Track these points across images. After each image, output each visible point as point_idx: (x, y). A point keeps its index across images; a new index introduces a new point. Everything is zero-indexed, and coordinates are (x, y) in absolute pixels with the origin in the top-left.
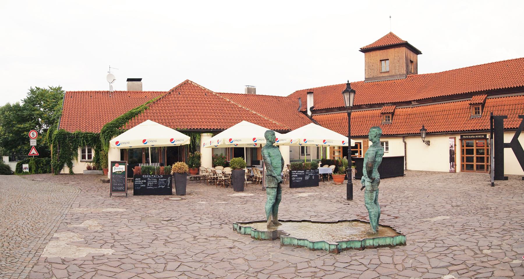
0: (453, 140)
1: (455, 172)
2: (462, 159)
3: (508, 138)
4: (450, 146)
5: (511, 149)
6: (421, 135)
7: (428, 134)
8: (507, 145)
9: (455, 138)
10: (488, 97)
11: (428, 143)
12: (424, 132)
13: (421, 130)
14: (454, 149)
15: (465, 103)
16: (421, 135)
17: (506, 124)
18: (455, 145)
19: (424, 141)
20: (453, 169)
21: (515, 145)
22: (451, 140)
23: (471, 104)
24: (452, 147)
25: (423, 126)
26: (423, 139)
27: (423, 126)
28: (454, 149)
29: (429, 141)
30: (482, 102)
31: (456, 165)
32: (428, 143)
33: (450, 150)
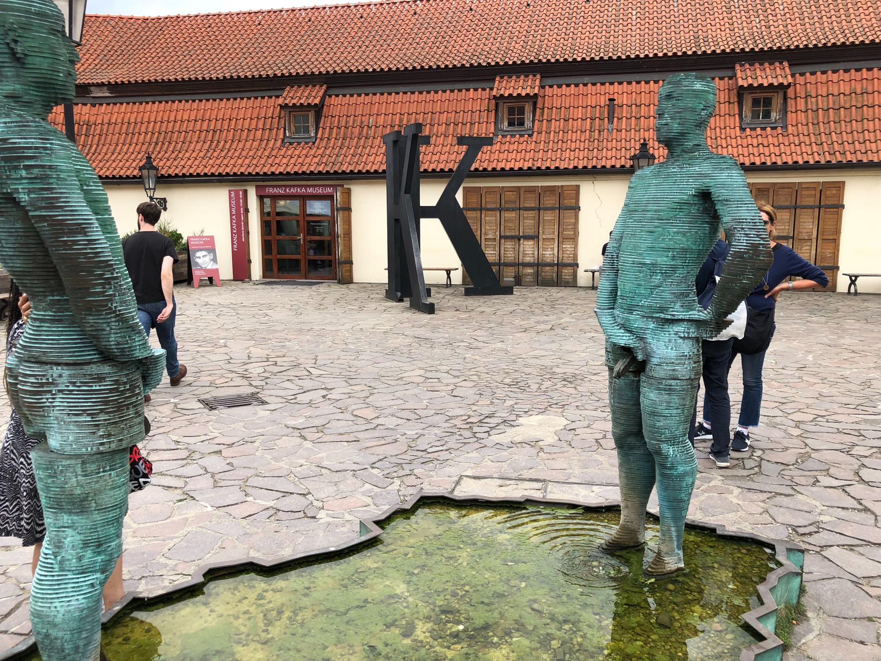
2: (267, 247)
3: (430, 195)
5: (436, 222)
6: (143, 183)
8: (429, 212)
9: (245, 192)
10: (330, 92)
12: (153, 173)
13: (141, 169)
15: (268, 106)
16: (143, 183)
17: (428, 159)
21: (445, 211)
23: (284, 107)
25: (149, 158)
26: (150, 193)
27: (149, 158)
29: (165, 200)
30: (317, 101)
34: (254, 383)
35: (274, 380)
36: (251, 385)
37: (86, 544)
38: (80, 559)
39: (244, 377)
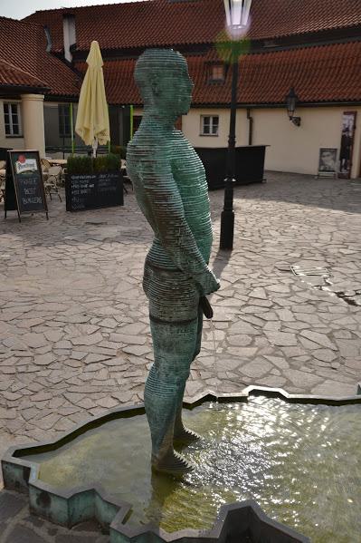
0: (352, 117)
1: (348, 177)
4: (342, 128)
7: (302, 105)
11: (297, 122)
12: (294, 99)
13: (287, 97)
14: (350, 134)
18: (354, 127)
19: (291, 118)
20: (344, 172)
22: (345, 116)
24: (347, 130)
25: (292, 90)
26: (291, 114)
28: (350, 134)
31: (351, 165)
32: (297, 122)
33: (343, 137)
34: (328, 260)
35: (344, 260)
36: (326, 261)
37: (170, 368)
38: (167, 375)
39: (323, 255)
